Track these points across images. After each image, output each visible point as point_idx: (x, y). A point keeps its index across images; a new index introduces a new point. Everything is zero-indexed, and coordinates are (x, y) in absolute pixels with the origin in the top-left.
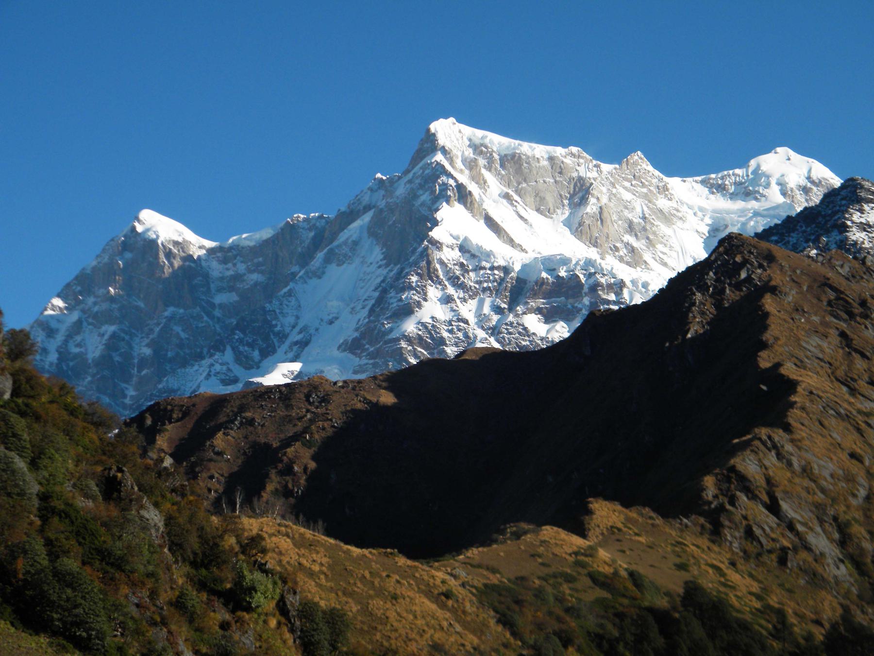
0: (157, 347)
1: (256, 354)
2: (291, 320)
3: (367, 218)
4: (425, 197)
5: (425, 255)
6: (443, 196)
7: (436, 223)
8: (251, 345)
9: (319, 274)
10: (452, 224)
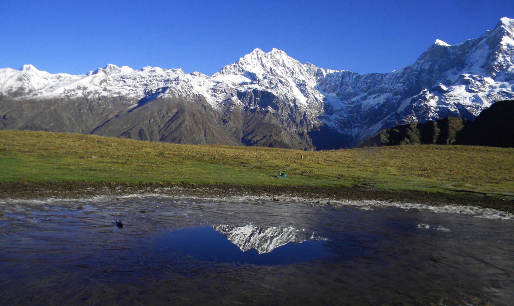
0: (439, 66)
1: (461, 68)
2: (468, 61)
3: (485, 40)
4: (499, 35)
5: (499, 47)
6: (503, 34)
7: (502, 40)
8: (460, 67)
9: (474, 52)
10: (505, 40)
